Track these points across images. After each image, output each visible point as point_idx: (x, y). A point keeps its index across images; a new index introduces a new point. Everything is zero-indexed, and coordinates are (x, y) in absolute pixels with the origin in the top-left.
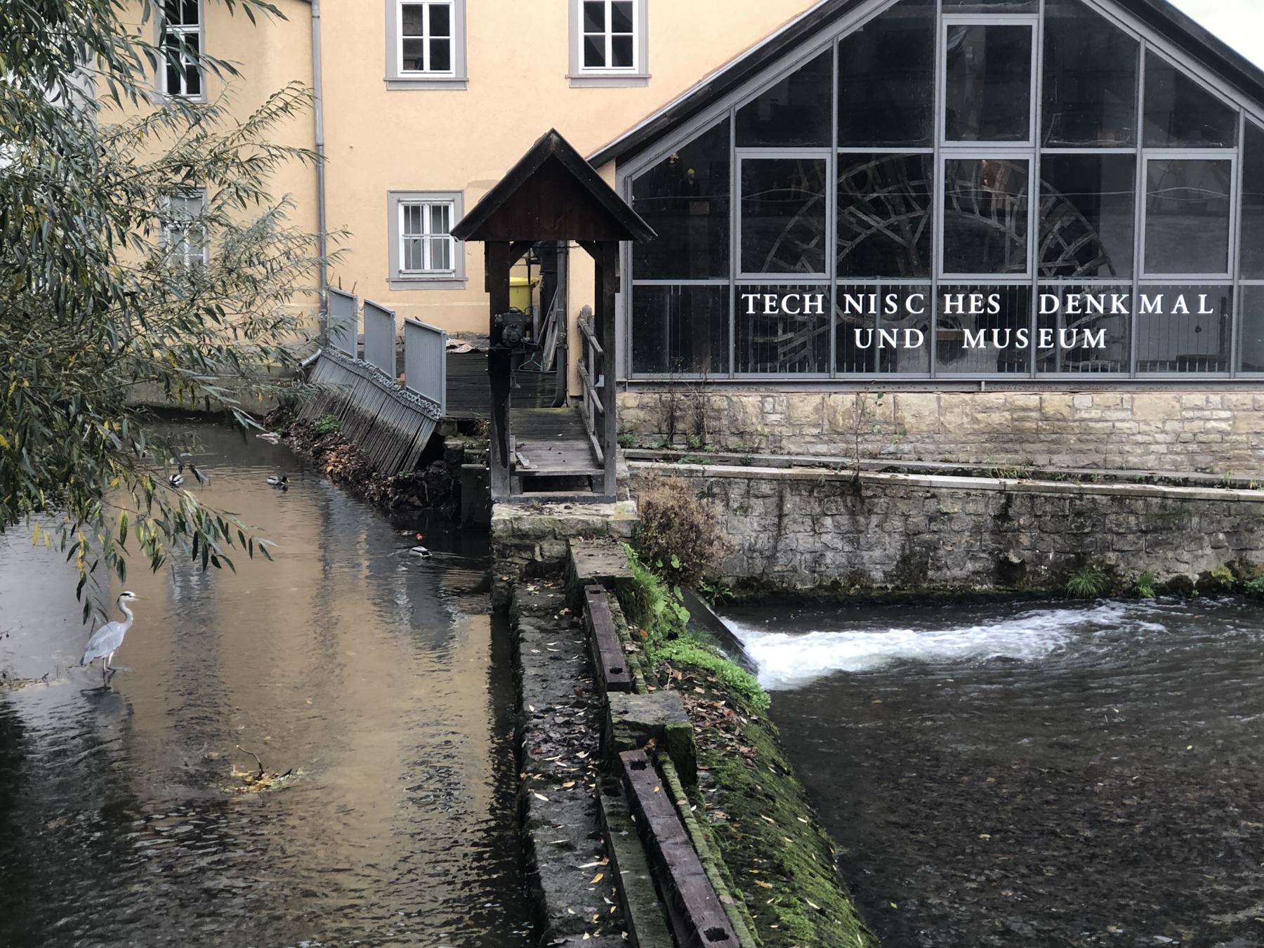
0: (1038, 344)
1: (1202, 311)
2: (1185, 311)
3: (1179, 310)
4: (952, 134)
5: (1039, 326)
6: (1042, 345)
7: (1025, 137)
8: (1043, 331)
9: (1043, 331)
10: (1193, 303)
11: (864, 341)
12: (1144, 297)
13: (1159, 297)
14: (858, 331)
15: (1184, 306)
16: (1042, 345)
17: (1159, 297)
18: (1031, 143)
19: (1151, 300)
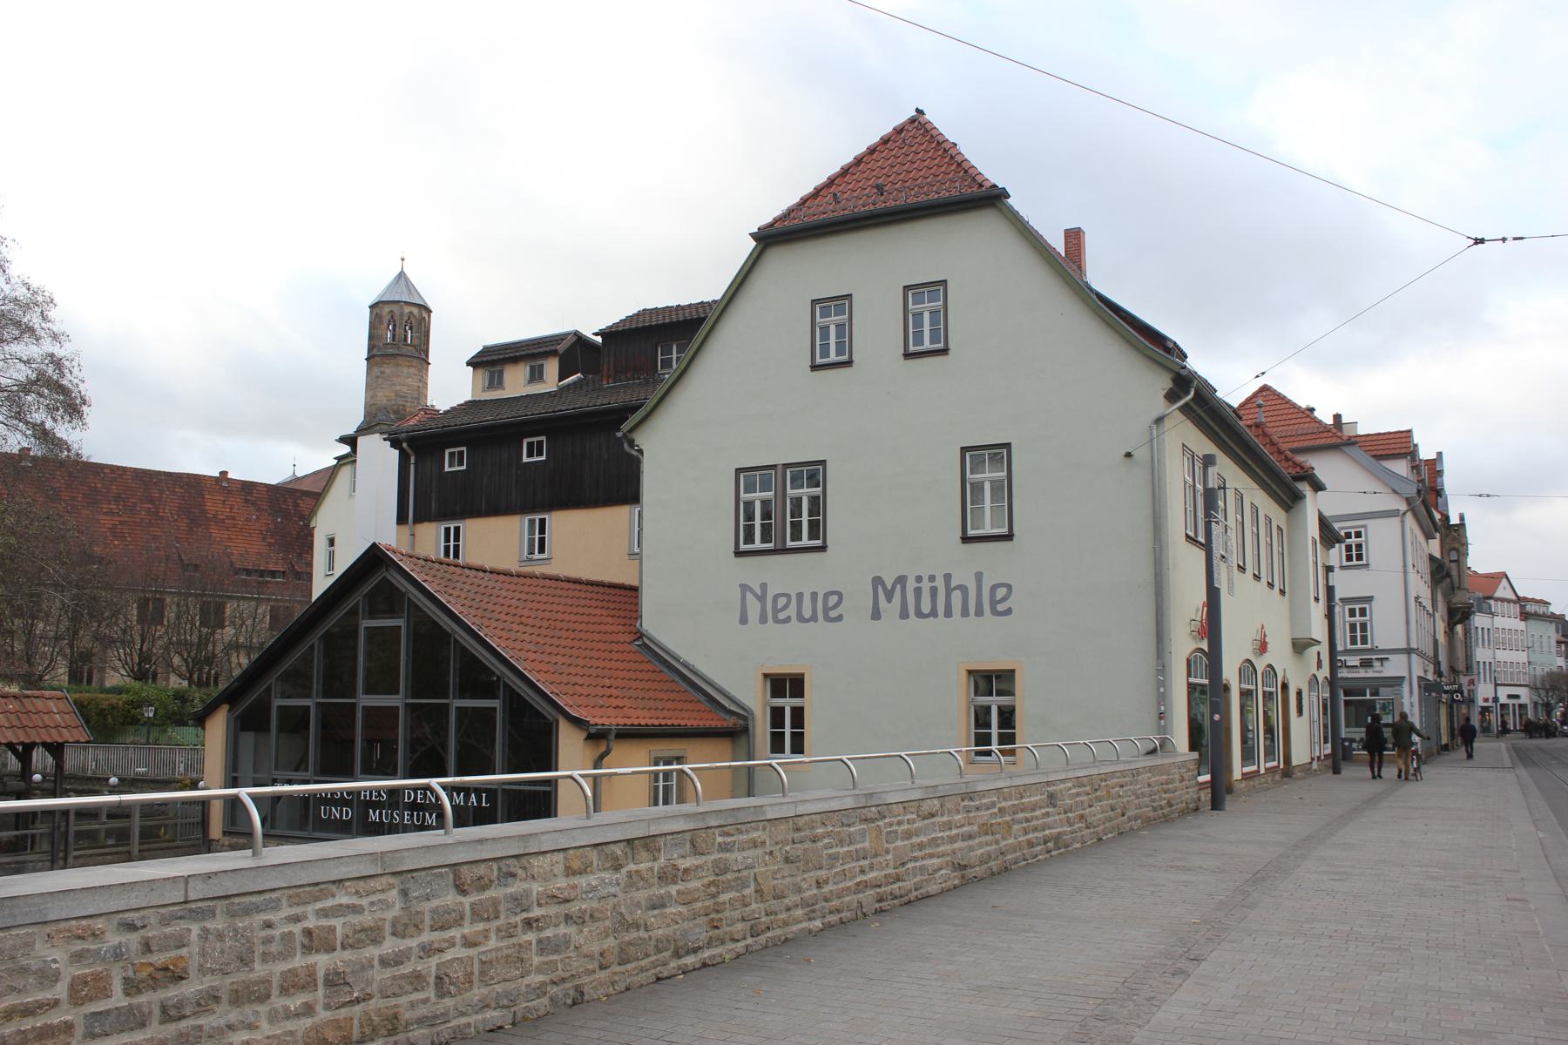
0: (404, 820)
1: (484, 805)
2: (475, 804)
3: (473, 803)
4: (370, 690)
5: (404, 810)
6: (406, 822)
7: (398, 693)
8: (406, 813)
9: (406, 813)
10: (479, 800)
11: (325, 815)
12: (455, 793)
13: (462, 794)
14: (323, 808)
15: (474, 800)
16: (406, 822)
17: (462, 794)
18: (400, 696)
19: (458, 797)
